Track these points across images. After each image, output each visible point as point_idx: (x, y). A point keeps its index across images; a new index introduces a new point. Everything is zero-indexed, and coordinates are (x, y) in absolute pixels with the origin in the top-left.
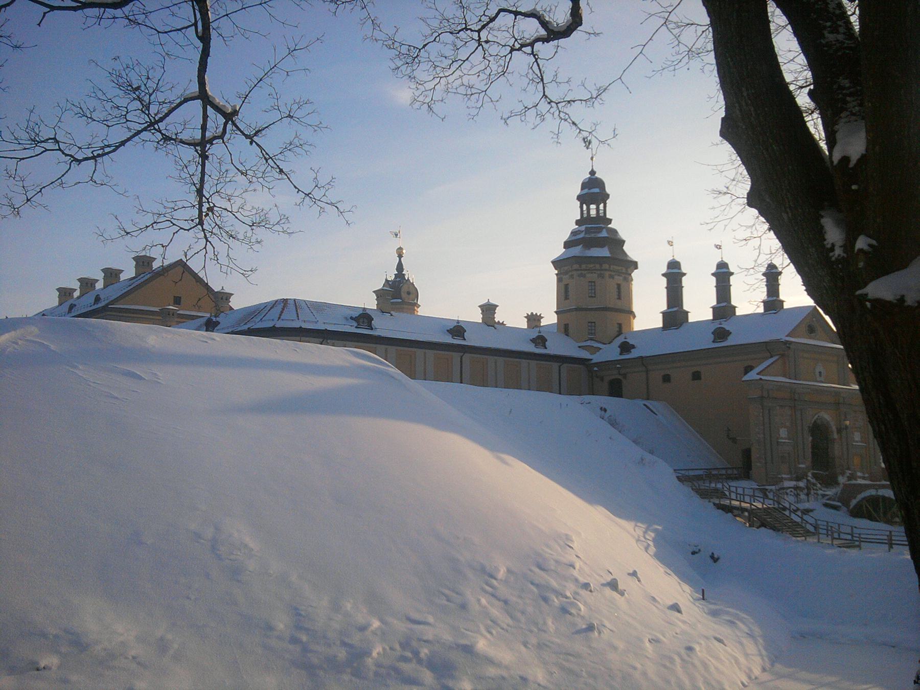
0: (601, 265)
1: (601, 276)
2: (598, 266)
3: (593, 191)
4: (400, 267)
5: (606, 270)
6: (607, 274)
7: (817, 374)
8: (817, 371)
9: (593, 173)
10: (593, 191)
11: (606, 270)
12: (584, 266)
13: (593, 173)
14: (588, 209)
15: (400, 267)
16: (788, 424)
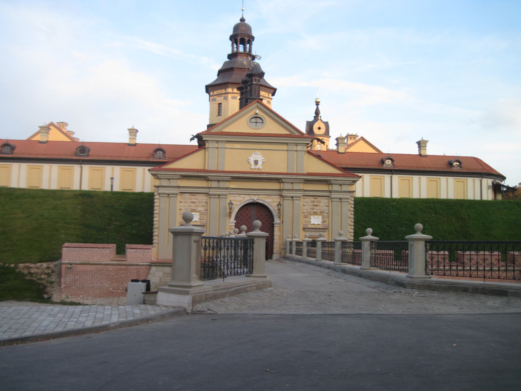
0: (226, 90)
1: (226, 98)
2: (224, 91)
3: (242, 36)
4: (317, 113)
5: (228, 93)
6: (230, 96)
7: (252, 163)
8: (252, 160)
9: (242, 20)
10: (242, 36)
11: (228, 93)
12: (215, 93)
13: (242, 20)
14: (237, 48)
15: (317, 113)
16: (200, 209)
